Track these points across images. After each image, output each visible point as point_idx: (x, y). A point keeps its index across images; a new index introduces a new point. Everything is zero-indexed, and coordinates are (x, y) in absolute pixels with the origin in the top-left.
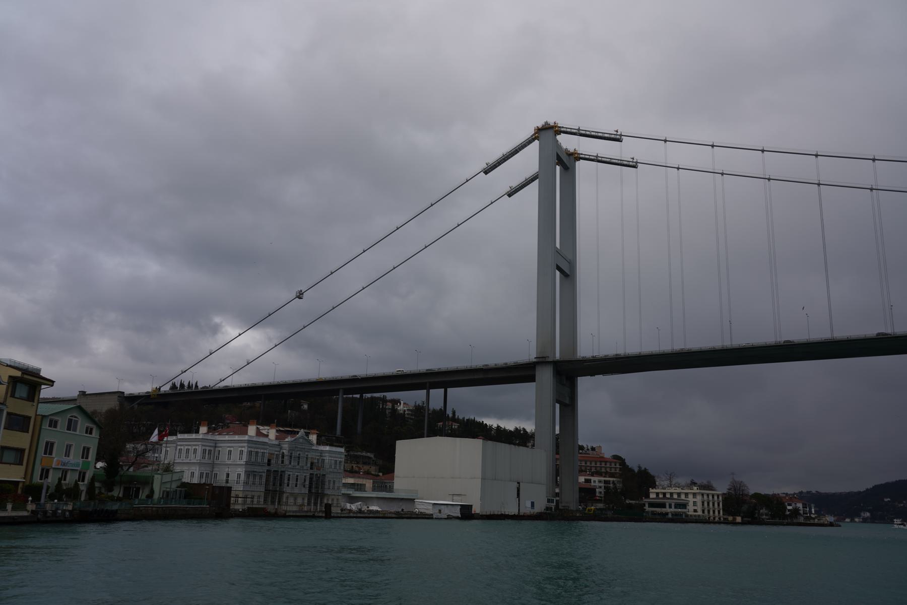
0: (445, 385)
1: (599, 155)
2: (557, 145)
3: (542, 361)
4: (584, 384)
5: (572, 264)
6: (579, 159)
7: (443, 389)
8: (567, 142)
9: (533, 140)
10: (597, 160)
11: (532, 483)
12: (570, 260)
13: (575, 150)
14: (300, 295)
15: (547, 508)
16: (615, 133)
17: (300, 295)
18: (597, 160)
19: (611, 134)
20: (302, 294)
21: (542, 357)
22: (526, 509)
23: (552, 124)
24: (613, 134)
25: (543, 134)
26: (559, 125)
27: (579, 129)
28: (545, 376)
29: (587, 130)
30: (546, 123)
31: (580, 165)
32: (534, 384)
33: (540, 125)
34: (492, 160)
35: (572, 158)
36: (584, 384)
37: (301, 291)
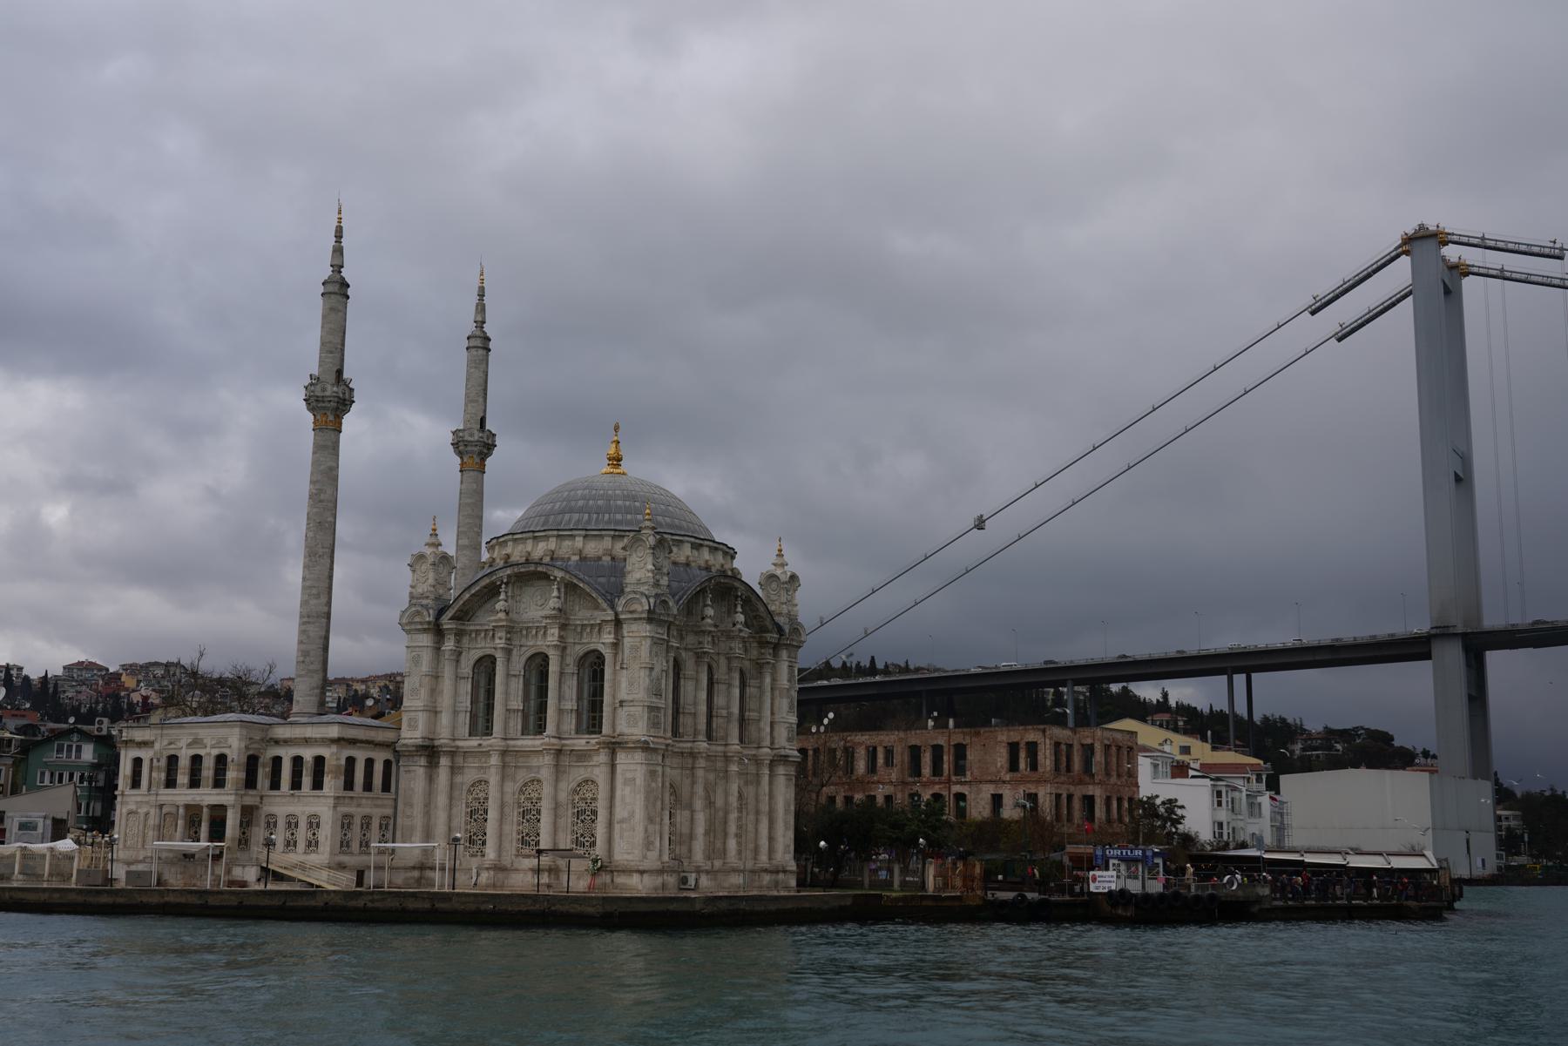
0: (1248, 671)
1: (1505, 268)
2: (1443, 259)
3: (1442, 633)
4: (1496, 660)
5: (1465, 459)
6: (1467, 274)
7: (1244, 676)
8: (1452, 253)
9: (1398, 256)
10: (1502, 275)
11: (1481, 831)
12: (1462, 453)
13: (1460, 258)
14: (980, 524)
15: (1499, 868)
16: (1552, 245)
17: (980, 524)
18: (1502, 275)
19: (1544, 247)
20: (984, 521)
21: (1444, 627)
22: (1478, 872)
23: (1433, 228)
24: (1547, 247)
25: (1417, 247)
26: (1446, 231)
27: (1483, 238)
28: (1452, 655)
29: (1498, 239)
30: (1421, 227)
31: (1468, 283)
32: (1425, 667)
33: (1410, 232)
34: (1325, 288)
35: (1455, 272)
36: (1496, 660)
37: (982, 516)
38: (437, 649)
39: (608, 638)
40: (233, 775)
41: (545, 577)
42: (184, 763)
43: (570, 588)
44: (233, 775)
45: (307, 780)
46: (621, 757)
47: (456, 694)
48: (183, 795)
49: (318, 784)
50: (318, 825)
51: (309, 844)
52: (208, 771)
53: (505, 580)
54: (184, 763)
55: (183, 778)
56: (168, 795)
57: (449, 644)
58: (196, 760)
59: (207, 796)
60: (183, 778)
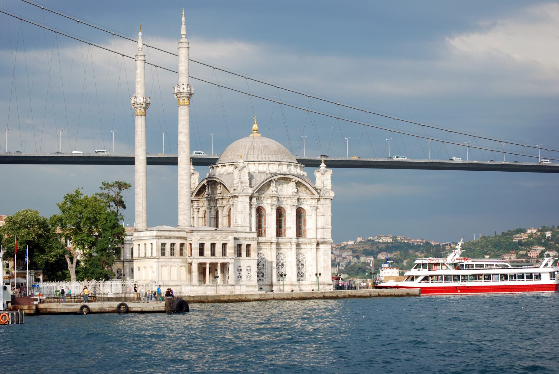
40: (230, 251)
41: (290, 180)
42: (207, 247)
43: (298, 184)
44: (230, 251)
46: (321, 246)
48: (208, 259)
49: (248, 255)
50: (250, 270)
51: (247, 277)
52: (218, 249)
53: (276, 180)
55: (207, 252)
57: (254, 201)
59: (219, 260)
60: (207, 252)
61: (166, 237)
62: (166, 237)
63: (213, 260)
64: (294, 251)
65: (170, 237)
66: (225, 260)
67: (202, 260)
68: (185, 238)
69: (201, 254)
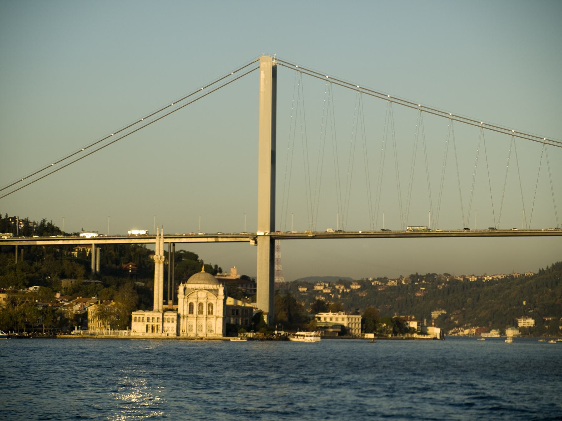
36: (277, 242)
38: (184, 301)
39: (215, 301)
40: (161, 320)
42: (151, 318)
45: (171, 321)
46: (218, 319)
47: (187, 308)
48: (150, 324)
49: (173, 322)
54: (151, 318)
56: (148, 323)
57: (186, 300)
58: (153, 318)
59: (155, 324)
60: (151, 321)
61: (136, 314)
62: (136, 314)
63: (153, 324)
64: (205, 320)
65: (138, 314)
66: (158, 324)
67: (148, 323)
68: (144, 315)
69: (148, 321)
